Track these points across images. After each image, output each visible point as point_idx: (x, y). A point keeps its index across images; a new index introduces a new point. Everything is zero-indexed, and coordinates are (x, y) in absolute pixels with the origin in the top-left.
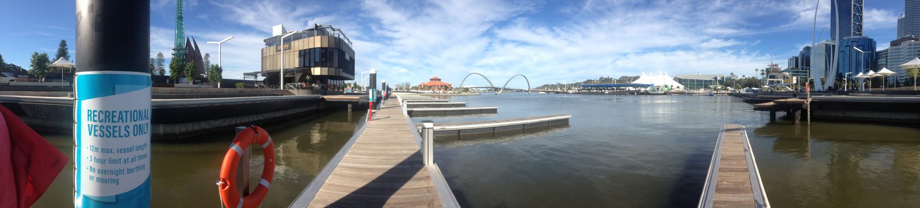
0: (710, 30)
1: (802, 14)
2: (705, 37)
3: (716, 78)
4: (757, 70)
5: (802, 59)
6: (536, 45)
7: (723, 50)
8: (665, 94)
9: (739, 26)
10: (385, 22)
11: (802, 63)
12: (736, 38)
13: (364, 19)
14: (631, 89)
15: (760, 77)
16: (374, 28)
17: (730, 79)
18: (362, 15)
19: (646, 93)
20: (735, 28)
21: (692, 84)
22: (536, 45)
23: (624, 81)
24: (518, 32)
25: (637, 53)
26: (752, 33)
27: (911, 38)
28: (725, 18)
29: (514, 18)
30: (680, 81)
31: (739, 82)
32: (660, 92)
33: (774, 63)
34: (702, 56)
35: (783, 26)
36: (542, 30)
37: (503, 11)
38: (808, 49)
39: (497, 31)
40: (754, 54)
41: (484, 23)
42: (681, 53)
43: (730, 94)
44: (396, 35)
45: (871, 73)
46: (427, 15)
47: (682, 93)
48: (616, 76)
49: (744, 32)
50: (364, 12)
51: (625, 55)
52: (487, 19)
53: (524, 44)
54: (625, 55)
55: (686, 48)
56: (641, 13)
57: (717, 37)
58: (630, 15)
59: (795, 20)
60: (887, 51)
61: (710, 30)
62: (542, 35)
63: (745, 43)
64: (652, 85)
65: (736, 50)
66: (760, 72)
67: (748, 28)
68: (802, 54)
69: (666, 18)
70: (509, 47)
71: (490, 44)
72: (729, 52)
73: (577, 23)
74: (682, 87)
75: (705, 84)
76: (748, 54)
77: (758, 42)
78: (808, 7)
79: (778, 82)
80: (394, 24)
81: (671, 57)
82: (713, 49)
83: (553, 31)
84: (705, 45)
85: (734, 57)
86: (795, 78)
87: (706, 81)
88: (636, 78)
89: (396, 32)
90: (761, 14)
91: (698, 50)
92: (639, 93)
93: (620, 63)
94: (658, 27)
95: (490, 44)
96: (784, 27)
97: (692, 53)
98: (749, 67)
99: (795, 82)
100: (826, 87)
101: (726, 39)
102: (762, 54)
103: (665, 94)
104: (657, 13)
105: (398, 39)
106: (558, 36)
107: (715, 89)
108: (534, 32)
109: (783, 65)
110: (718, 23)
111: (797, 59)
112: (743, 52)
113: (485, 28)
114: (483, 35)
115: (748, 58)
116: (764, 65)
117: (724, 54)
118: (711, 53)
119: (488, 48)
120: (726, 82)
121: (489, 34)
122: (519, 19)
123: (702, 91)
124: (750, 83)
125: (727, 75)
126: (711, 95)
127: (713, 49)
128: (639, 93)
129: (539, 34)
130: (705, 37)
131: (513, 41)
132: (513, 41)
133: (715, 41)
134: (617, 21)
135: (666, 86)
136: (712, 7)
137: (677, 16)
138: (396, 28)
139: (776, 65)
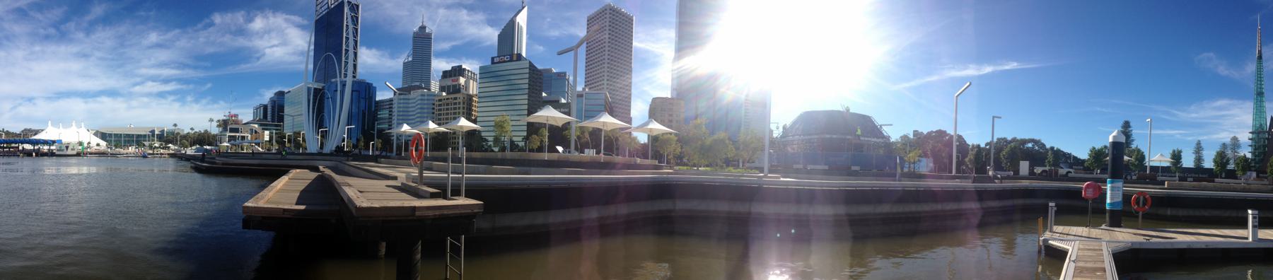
0: (144, 71)
1: (268, 51)
2: (138, 80)
3: (153, 132)
4: (211, 120)
5: (273, 108)
7: (161, 95)
8: (78, 155)
9: (182, 66)
11: (273, 113)
12: (179, 80)
14: (28, 147)
15: (215, 130)
17: (173, 133)
19: (51, 154)
20: (178, 68)
21: (117, 140)
23: (26, 136)
25: (49, 98)
26: (200, 74)
27: (420, 87)
28: (164, 55)
30: (103, 136)
31: (186, 137)
32: (70, 152)
33: (233, 112)
34: (134, 103)
35: (243, 66)
38: (281, 94)
40: (204, 101)
42: (105, 99)
43: (172, 156)
45: (432, 126)
47: (102, 154)
48: (16, 128)
49: (190, 73)
51: (30, 99)
54: (30, 99)
55: (112, 93)
56: (51, 48)
57: (153, 79)
58: (37, 48)
59: (258, 59)
60: (391, 100)
61: (144, 71)
63: (191, 86)
64: (60, 142)
65: (180, 96)
66: (215, 124)
67: (195, 68)
68: (273, 101)
69: (85, 56)
72: (172, 98)
74: (103, 144)
75: (137, 140)
76: (196, 101)
77: (209, 85)
78: (275, 42)
79: (243, 138)
81: (93, 105)
82: (149, 95)
84: (137, 88)
85: (177, 105)
86: (267, 133)
87: (139, 136)
88: (37, 132)
90: (211, 50)
91: (130, 96)
92: (40, 154)
93: (24, 110)
94: (76, 66)
96: (244, 68)
97: (120, 99)
98: (199, 117)
99: (267, 138)
100: (330, 146)
101: (166, 81)
102: (215, 101)
103: (78, 155)
104: (74, 49)
107: (151, 147)
109: (246, 115)
110: (153, 61)
111: (265, 107)
112: (189, 99)
115: (196, 107)
116: (221, 116)
117: (163, 101)
118: (145, 100)
120: (167, 138)
123: (132, 149)
124: (201, 139)
125: (168, 127)
126: (145, 157)
127: (149, 95)
128: (40, 154)
130: (138, 80)
133: (150, 83)
134: (19, 54)
135: (81, 144)
136: (145, 42)
137: (98, 54)
139: (236, 116)
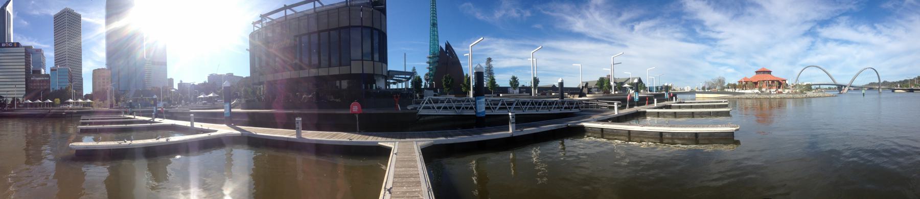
6: (858, 43)
10: (707, 24)
13: (687, 20)
16: (698, 30)
18: (685, 17)
22: (858, 43)
24: (841, 31)
29: (837, 17)
36: (864, 28)
37: (825, 10)
39: (819, 30)
41: (806, 22)
44: (720, 36)
46: (750, 14)
50: (685, 14)
52: (809, 19)
53: (847, 42)
62: (864, 33)
70: (830, 45)
71: (813, 43)
73: (900, 17)
80: (716, 25)
83: (875, 28)
89: (719, 32)
95: (813, 43)
105: (721, 39)
106: (880, 32)
108: (856, 30)
113: (807, 27)
114: (806, 34)
119: (811, 48)
121: (810, 33)
122: (841, 18)
129: (861, 32)
131: (836, 40)
132: (836, 40)
138: (718, 29)
